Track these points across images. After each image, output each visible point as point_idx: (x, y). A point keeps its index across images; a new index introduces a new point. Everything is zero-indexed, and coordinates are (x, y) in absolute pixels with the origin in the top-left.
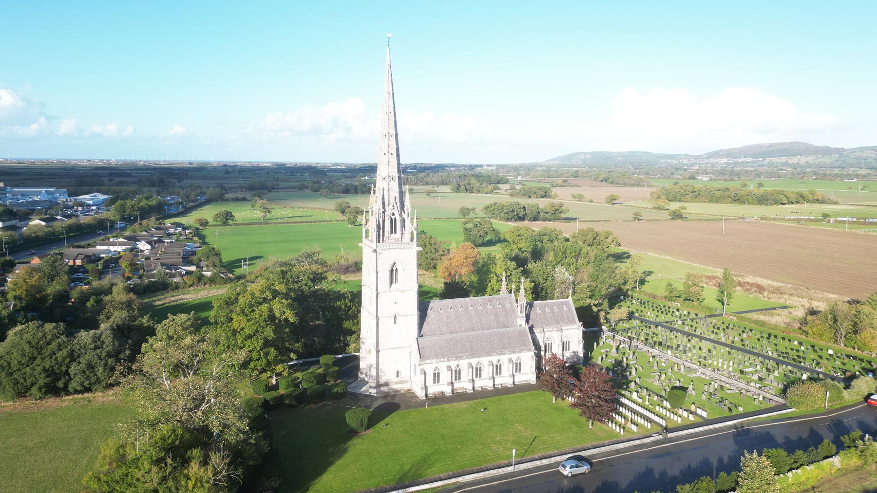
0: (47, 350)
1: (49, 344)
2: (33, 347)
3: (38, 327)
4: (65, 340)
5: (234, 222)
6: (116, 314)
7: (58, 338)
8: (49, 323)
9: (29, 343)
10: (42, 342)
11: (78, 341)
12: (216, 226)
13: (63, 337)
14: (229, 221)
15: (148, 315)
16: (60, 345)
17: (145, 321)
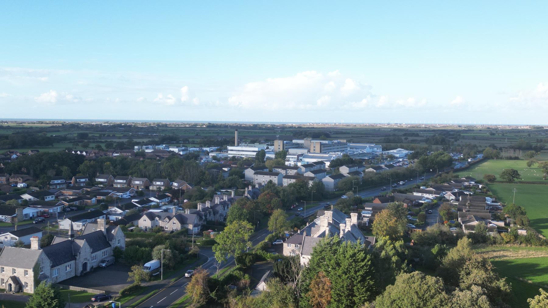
0: (431, 303)
1: (432, 297)
2: (420, 298)
3: (422, 278)
4: (446, 297)
5: (519, 180)
6: (475, 271)
7: (440, 293)
8: (430, 276)
9: (417, 292)
10: (427, 295)
11: (457, 301)
12: (502, 182)
13: (444, 293)
14: (515, 179)
15: (504, 279)
16: (442, 301)
17: (502, 284)
